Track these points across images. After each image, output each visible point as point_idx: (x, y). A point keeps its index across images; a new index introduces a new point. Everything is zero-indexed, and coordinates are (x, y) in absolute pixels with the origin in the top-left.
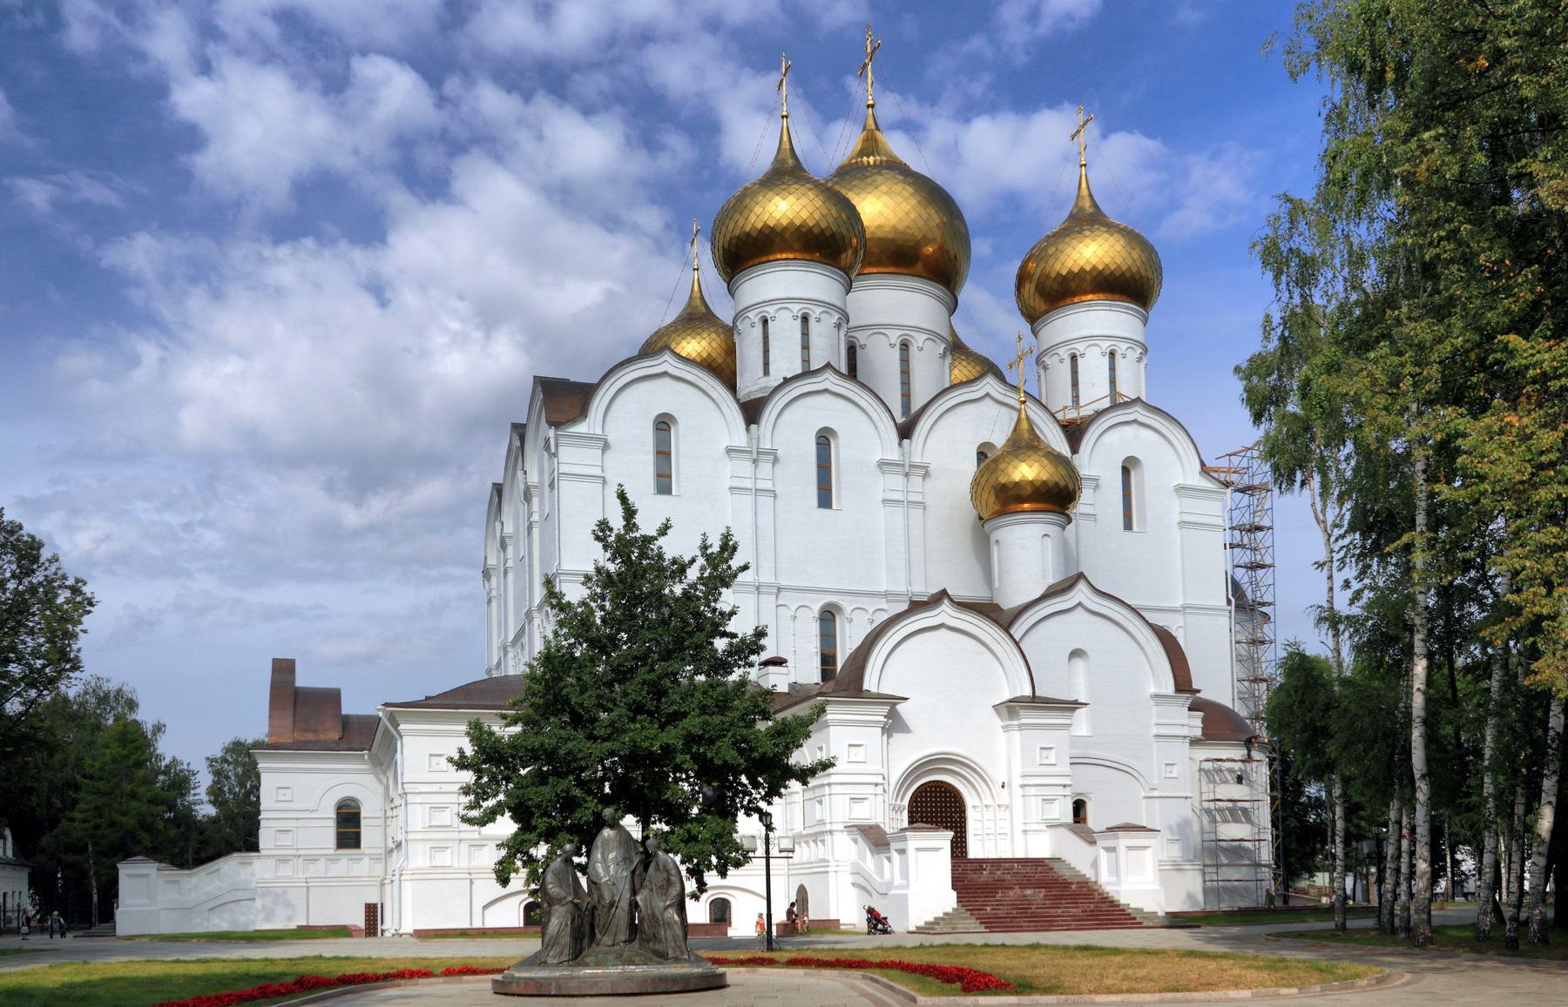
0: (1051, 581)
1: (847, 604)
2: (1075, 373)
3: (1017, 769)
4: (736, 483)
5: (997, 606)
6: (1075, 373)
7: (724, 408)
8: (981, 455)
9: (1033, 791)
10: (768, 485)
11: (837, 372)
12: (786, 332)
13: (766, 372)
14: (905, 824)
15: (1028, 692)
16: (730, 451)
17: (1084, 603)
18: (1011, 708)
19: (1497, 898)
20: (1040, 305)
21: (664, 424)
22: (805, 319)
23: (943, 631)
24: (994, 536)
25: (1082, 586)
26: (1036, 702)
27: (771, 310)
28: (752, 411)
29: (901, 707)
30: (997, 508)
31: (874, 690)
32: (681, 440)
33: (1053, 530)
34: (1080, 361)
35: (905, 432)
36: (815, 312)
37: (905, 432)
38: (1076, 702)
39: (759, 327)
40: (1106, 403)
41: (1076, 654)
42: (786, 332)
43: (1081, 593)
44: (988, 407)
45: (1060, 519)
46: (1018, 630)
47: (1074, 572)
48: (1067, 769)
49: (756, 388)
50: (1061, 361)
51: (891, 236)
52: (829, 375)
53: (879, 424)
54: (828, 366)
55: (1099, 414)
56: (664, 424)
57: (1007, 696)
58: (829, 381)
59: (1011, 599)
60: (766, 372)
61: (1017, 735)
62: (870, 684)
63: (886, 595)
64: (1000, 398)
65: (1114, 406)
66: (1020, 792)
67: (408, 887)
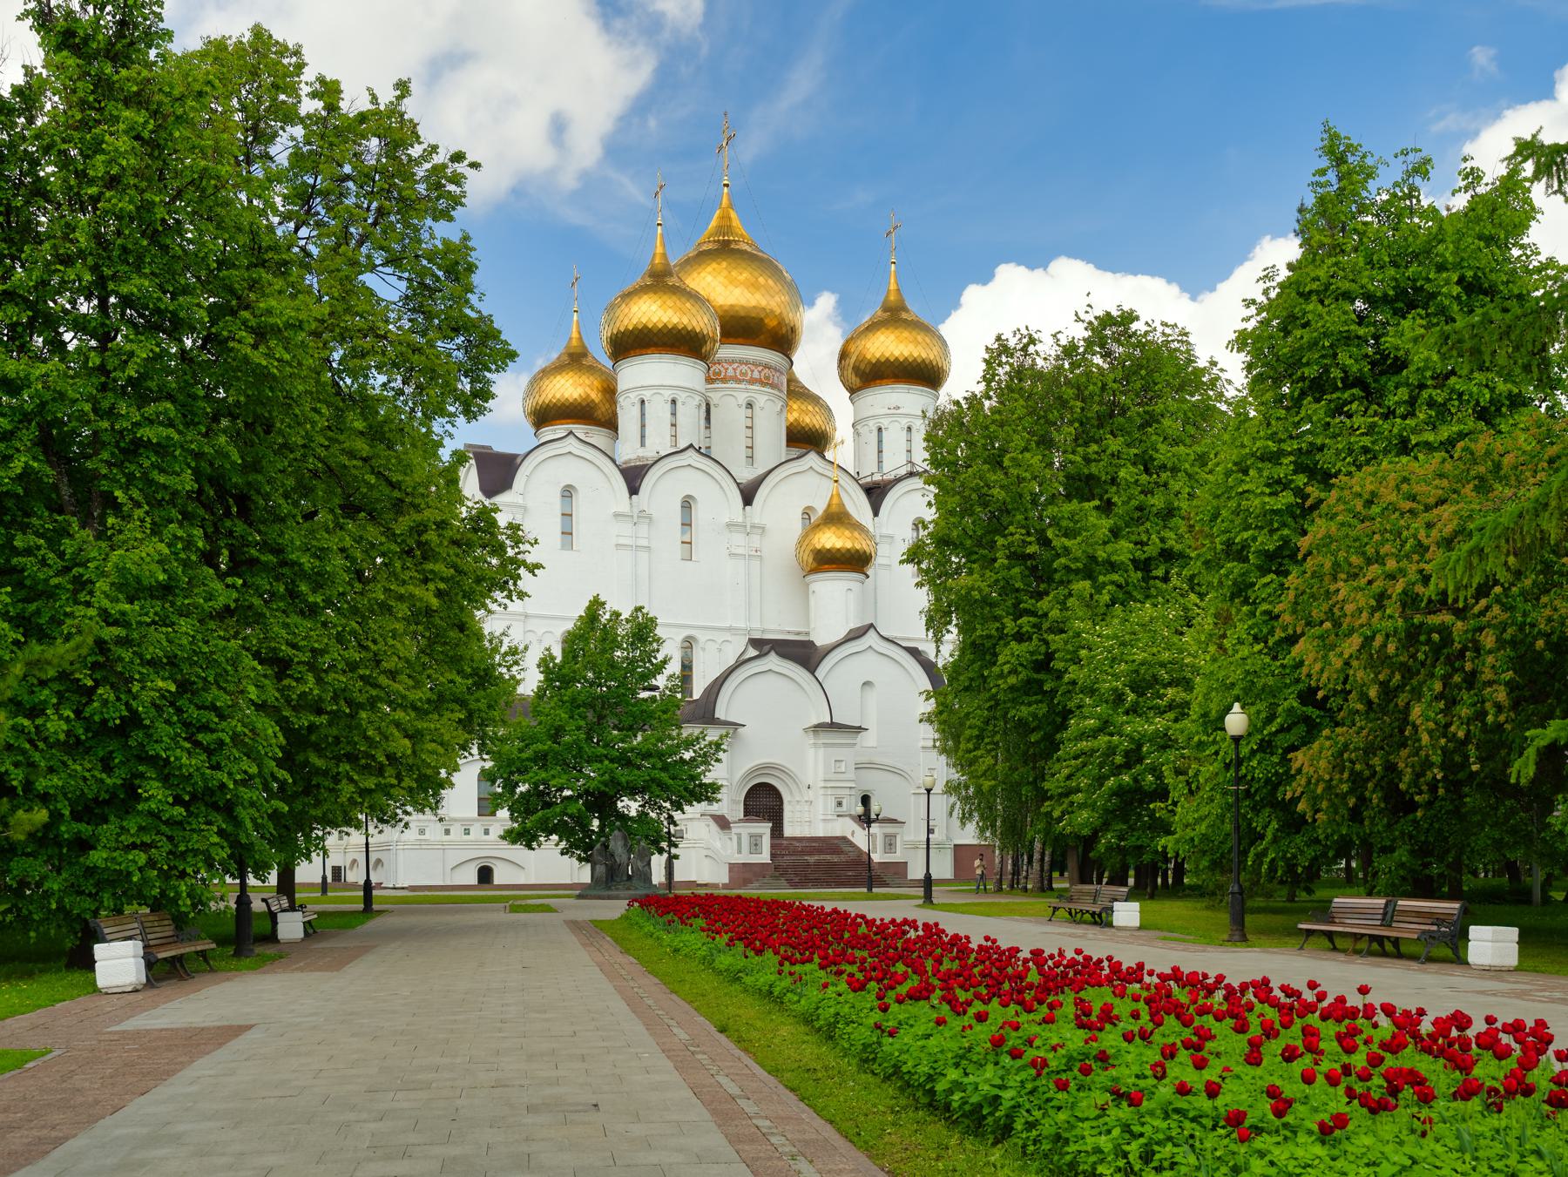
0: (852, 626)
1: (701, 637)
2: (880, 441)
3: (821, 776)
4: (622, 541)
5: (811, 643)
6: (880, 441)
7: (612, 480)
8: (807, 513)
9: (829, 792)
10: (646, 544)
11: (698, 451)
12: (658, 412)
13: (643, 444)
14: (742, 816)
15: (828, 720)
16: (617, 515)
17: (874, 646)
18: (819, 728)
19: (1159, 880)
20: (856, 381)
21: (568, 492)
22: (674, 402)
23: (770, 674)
24: (813, 587)
25: (871, 633)
26: (833, 726)
27: (647, 395)
28: (634, 477)
29: (741, 730)
30: (815, 565)
31: (722, 717)
32: (581, 507)
33: (855, 586)
34: (884, 432)
35: (748, 495)
36: (681, 397)
37: (748, 495)
38: (860, 728)
39: (638, 406)
40: (903, 471)
41: (867, 684)
42: (658, 412)
43: (871, 639)
44: (811, 478)
45: (862, 576)
46: (821, 672)
47: (867, 622)
48: (851, 775)
49: (633, 456)
50: (871, 432)
51: (742, 313)
52: (691, 452)
53: (728, 492)
54: (691, 446)
55: (898, 480)
56: (568, 492)
57: (815, 722)
58: (691, 457)
59: (821, 639)
60: (643, 444)
61: (821, 751)
62: (720, 713)
63: (729, 629)
64: (821, 471)
65: (911, 474)
66: (822, 792)
67: (401, 853)
